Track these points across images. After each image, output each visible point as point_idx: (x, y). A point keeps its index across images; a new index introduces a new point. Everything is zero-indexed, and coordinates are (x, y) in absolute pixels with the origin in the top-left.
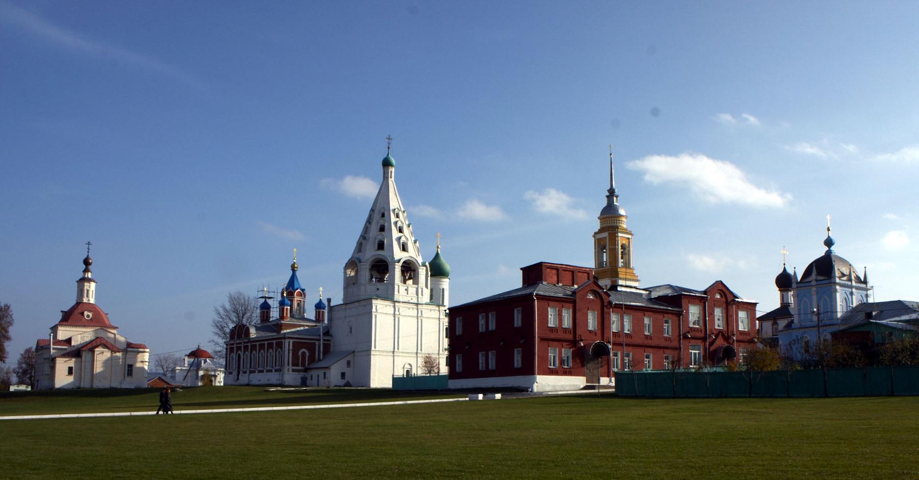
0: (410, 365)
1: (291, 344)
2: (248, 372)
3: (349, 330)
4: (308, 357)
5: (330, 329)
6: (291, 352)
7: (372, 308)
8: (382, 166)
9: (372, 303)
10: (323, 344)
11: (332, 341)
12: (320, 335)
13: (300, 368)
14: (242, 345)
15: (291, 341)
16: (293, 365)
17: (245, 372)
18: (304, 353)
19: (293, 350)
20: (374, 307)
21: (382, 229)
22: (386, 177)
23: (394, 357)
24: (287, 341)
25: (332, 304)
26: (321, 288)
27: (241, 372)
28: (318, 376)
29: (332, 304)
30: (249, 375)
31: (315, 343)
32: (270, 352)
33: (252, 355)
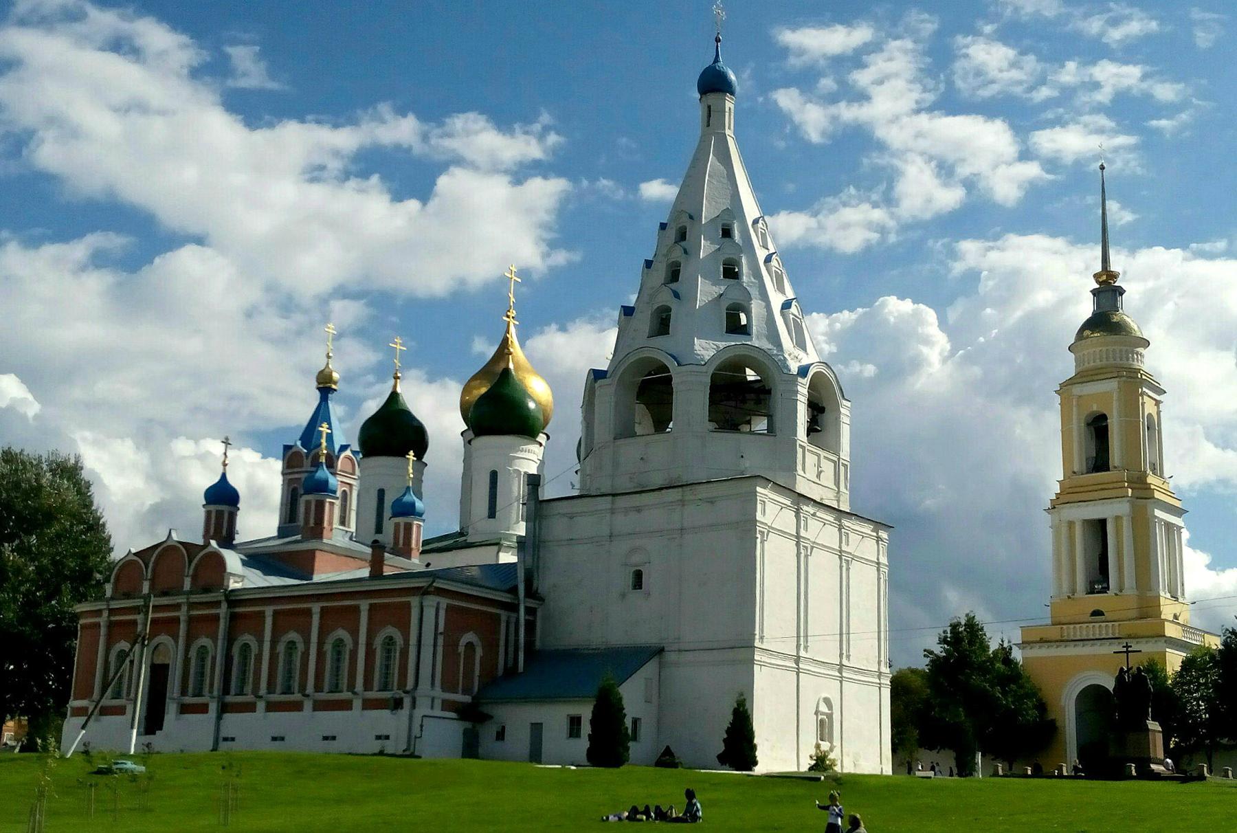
0: (827, 702)
1: (442, 614)
2: (213, 707)
3: (630, 581)
5: (536, 576)
7: (756, 511)
10: (526, 620)
11: (539, 614)
12: (514, 590)
14: (182, 614)
15: (444, 602)
17: (185, 709)
20: (759, 507)
21: (731, 272)
22: (712, 117)
23: (798, 674)
24: (431, 601)
25: (547, 492)
26: (411, 453)
28: (537, 728)
29: (547, 492)
30: (219, 718)
31: (499, 616)
33: (281, 648)
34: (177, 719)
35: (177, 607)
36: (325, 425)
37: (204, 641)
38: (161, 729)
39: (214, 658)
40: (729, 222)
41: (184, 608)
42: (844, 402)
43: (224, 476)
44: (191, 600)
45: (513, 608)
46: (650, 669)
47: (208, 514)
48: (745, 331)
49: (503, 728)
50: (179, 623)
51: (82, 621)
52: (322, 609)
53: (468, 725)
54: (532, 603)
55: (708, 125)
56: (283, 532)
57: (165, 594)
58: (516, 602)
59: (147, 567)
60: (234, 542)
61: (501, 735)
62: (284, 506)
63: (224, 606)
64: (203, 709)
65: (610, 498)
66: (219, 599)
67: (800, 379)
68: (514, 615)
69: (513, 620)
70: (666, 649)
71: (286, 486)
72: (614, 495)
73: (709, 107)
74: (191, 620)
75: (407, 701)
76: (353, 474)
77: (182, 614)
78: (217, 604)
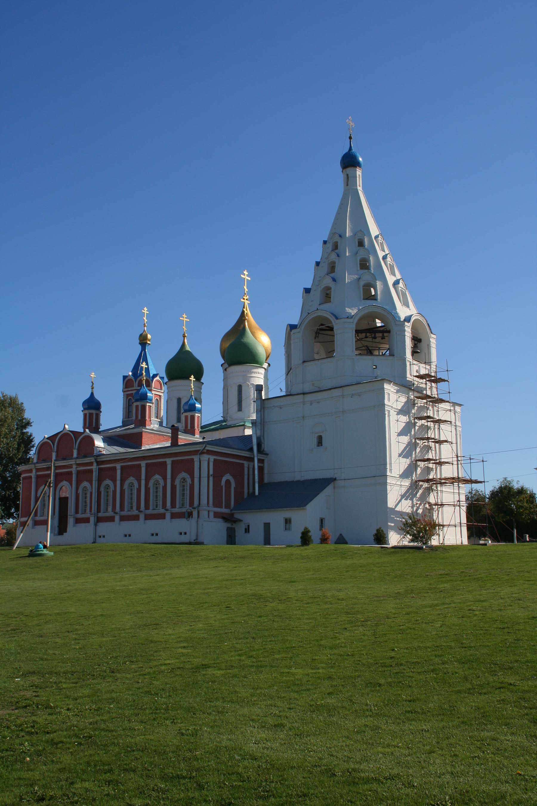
1: (211, 464)
2: (92, 519)
3: (315, 441)
4: (235, 488)
6: (211, 479)
8: (340, 169)
9: (383, 389)
10: (259, 467)
11: (266, 461)
12: (251, 450)
13: (224, 510)
15: (212, 458)
16: (215, 505)
17: (78, 521)
18: (228, 482)
19: (214, 476)
20: (386, 396)
21: (364, 265)
22: (349, 181)
24: (205, 457)
26: (192, 376)
27: (71, 521)
28: (267, 526)
30: (96, 525)
31: (243, 464)
32: (85, 488)
34: (74, 526)
35: (70, 466)
36: (144, 363)
37: (86, 484)
38: (66, 532)
39: (91, 493)
40: (362, 238)
41: (74, 466)
42: (432, 335)
43: (92, 394)
44: (78, 462)
45: (251, 459)
46: (329, 490)
47: (85, 415)
48: (374, 298)
49: (249, 526)
50: (72, 474)
51: (23, 476)
52: (147, 464)
53: (229, 525)
54: (262, 457)
55: (347, 185)
56: (125, 424)
57: (64, 459)
58: (252, 456)
59: (54, 445)
60: (100, 430)
61: (247, 530)
62: (125, 409)
63: (95, 464)
64: (87, 520)
65: (302, 395)
66: (92, 461)
67: (406, 324)
68: (252, 464)
69: (251, 466)
70: (337, 479)
71: (125, 398)
72: (304, 394)
73: (347, 175)
74: (78, 473)
75: (195, 514)
76: (161, 389)
77: (74, 470)
78: (91, 464)
